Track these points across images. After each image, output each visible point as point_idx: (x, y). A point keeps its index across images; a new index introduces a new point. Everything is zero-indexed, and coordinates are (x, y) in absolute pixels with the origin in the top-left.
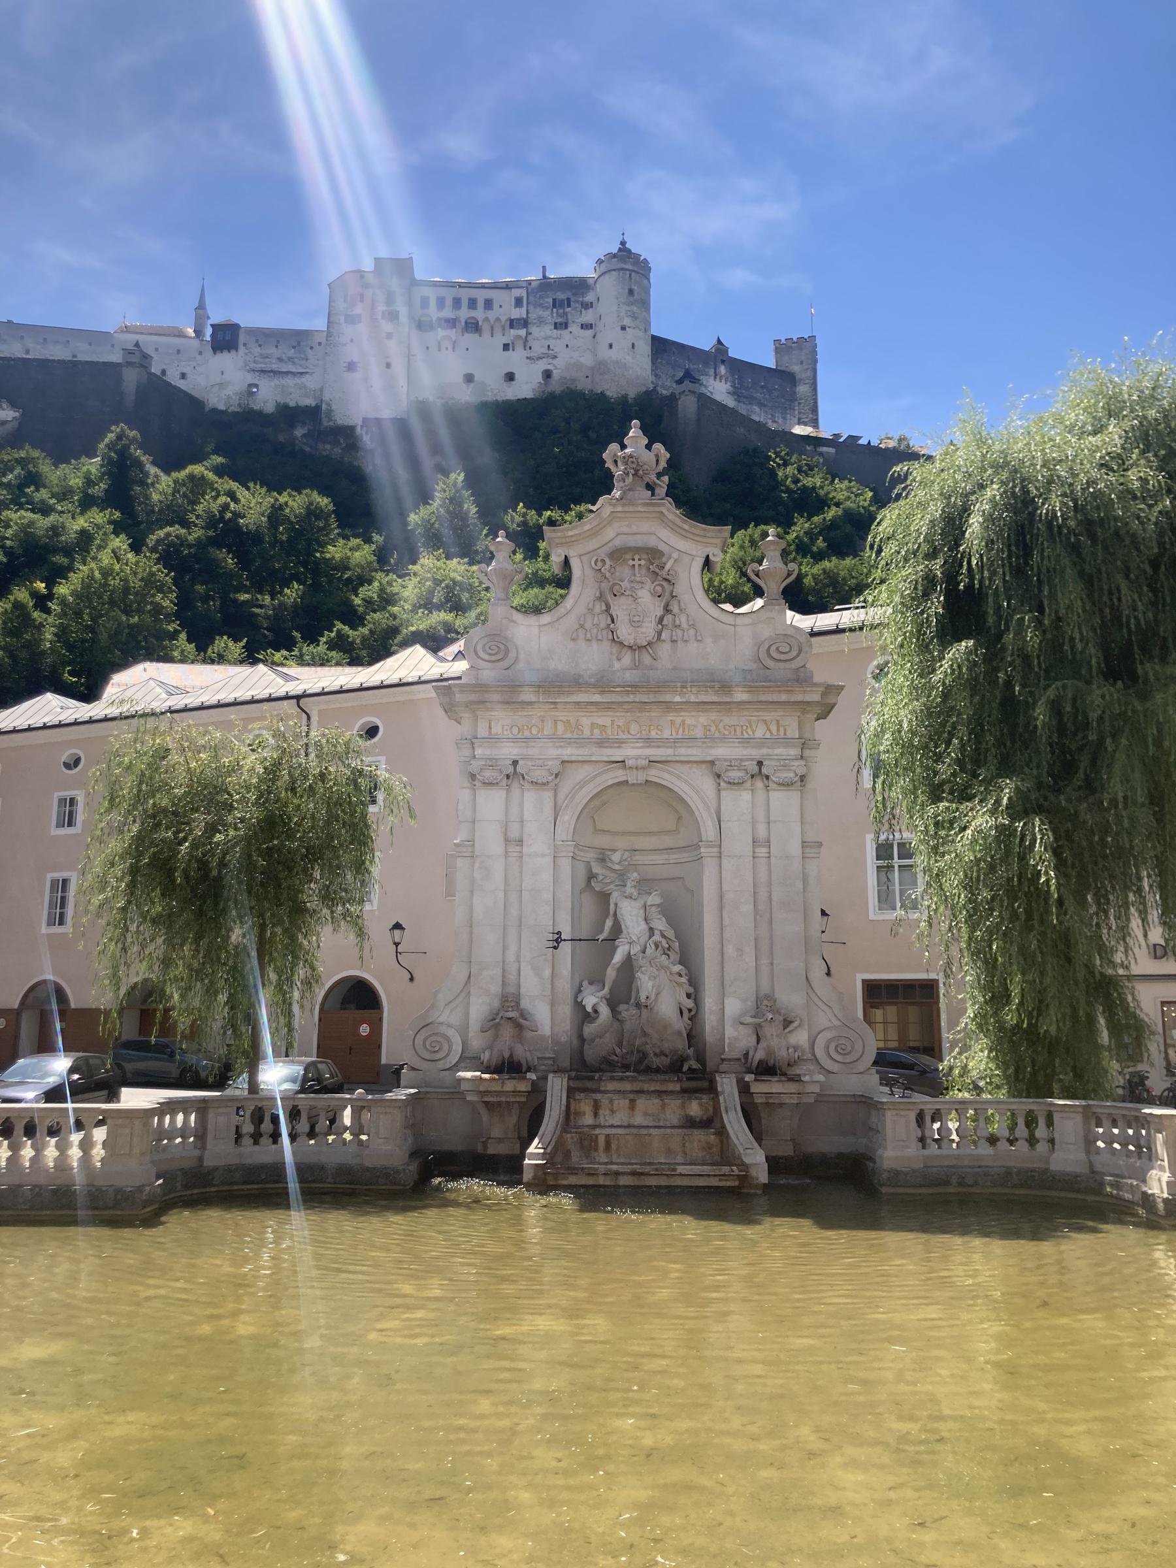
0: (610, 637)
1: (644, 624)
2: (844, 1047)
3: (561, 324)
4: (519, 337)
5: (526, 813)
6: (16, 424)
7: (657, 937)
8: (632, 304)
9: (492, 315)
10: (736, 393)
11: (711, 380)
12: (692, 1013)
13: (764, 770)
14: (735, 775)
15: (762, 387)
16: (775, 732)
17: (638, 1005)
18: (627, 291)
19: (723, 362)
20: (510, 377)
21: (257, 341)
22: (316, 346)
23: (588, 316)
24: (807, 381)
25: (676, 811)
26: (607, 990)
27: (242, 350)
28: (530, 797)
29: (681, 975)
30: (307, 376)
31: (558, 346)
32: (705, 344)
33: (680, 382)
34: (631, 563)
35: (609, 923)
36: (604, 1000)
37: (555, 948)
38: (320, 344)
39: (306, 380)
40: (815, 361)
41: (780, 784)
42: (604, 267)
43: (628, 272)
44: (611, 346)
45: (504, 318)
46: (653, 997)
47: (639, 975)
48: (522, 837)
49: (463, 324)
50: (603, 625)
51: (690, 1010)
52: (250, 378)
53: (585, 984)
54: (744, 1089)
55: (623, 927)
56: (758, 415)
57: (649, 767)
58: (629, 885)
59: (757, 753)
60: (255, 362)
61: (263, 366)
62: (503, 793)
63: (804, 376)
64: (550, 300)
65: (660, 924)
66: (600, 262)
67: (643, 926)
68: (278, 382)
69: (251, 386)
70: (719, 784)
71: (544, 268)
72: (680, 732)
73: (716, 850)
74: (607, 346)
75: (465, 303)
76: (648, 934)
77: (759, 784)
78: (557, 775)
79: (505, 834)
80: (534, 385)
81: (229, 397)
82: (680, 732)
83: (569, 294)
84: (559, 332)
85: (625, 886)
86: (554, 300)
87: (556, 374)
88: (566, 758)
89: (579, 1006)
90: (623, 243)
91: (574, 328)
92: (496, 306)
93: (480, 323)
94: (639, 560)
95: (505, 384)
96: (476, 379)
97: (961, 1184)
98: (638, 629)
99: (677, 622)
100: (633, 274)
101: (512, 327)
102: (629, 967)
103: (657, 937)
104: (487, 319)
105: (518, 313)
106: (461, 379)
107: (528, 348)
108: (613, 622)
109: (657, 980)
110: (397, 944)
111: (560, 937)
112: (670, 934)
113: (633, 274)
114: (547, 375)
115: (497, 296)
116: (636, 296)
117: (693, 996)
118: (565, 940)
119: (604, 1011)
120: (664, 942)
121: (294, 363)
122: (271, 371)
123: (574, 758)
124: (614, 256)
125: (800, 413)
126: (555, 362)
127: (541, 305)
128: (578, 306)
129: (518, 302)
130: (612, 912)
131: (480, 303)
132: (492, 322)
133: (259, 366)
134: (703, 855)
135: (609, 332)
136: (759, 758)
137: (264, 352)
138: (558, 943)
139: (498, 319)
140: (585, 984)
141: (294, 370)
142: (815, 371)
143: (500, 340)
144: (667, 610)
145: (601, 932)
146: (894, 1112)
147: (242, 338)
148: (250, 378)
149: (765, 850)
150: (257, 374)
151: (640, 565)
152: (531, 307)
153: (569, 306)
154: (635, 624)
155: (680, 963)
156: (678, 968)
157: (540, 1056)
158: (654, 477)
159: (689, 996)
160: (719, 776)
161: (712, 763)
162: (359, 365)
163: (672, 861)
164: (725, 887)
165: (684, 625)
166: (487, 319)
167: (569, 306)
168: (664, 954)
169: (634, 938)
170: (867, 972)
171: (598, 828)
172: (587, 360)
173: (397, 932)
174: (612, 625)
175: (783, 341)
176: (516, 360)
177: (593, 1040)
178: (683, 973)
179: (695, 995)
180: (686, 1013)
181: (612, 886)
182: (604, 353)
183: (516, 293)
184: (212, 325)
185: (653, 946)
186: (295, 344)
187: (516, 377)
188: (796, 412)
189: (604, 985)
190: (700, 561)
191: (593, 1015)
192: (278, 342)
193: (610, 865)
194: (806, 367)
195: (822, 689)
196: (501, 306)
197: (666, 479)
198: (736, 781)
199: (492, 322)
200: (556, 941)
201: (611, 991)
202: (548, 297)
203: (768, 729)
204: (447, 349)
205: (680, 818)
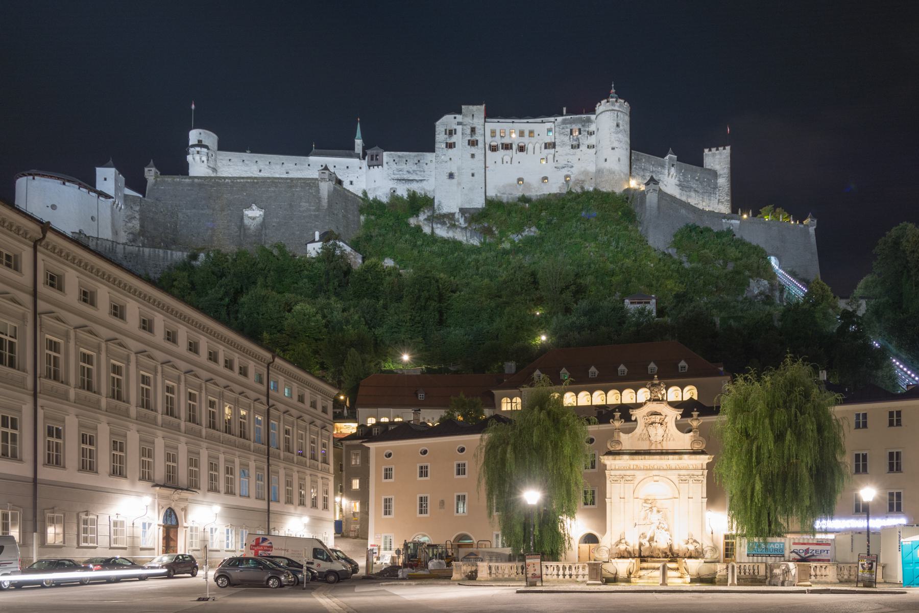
6: (262, 219)
8: (617, 133)
9: (533, 140)
10: (682, 186)
11: (666, 177)
15: (697, 180)
18: (615, 124)
21: (394, 161)
23: (592, 140)
24: (724, 176)
30: (425, 182)
31: (573, 160)
39: (424, 184)
44: (606, 160)
52: (393, 185)
60: (394, 174)
61: (398, 176)
63: (722, 172)
64: (569, 130)
68: (408, 187)
80: (560, 185)
81: (380, 196)
83: (580, 126)
91: (583, 148)
92: (536, 134)
101: (546, 148)
106: (516, 182)
116: (621, 127)
121: (417, 174)
122: (403, 180)
126: (572, 170)
131: (527, 133)
133: (396, 177)
135: (606, 152)
137: (398, 167)
148: (393, 185)
152: (557, 135)
172: (592, 168)
192: (407, 161)
202: (567, 128)
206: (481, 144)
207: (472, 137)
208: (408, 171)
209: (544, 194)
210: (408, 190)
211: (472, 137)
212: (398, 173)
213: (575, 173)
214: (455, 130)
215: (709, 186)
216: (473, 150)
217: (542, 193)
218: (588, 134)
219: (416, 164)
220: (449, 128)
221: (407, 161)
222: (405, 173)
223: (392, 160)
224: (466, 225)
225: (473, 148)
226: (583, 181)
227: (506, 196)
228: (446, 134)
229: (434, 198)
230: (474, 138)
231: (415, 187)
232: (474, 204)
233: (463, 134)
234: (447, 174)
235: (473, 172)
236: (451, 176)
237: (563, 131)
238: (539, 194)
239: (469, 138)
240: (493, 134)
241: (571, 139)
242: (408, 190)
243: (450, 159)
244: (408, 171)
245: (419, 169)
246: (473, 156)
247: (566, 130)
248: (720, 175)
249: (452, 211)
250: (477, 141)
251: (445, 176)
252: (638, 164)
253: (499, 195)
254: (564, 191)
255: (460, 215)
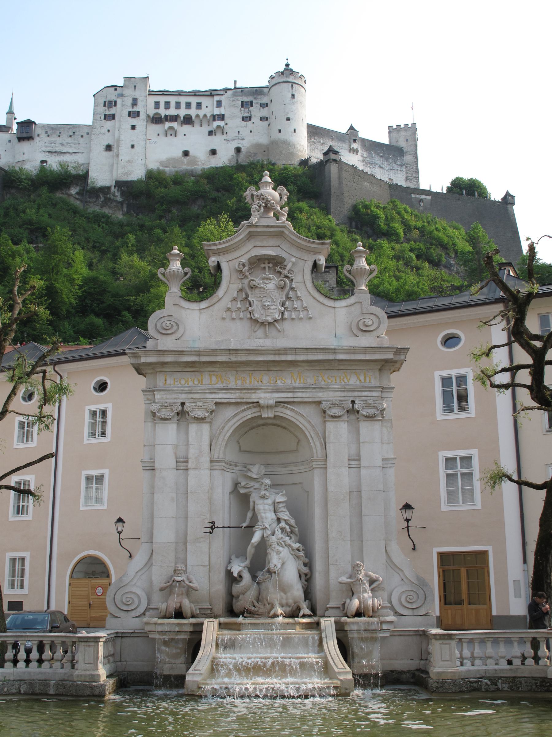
0: (249, 316)
1: (272, 307)
2: (411, 597)
3: (247, 117)
4: (219, 127)
5: (190, 439)
7: (283, 524)
12: (308, 577)
13: (356, 406)
14: (335, 411)
16: (363, 381)
17: (270, 572)
19: (355, 141)
20: (213, 152)
21: (47, 132)
22: (85, 135)
23: (264, 112)
24: (411, 153)
25: (296, 437)
26: (247, 562)
27: (37, 139)
28: (193, 428)
29: (298, 550)
30: (79, 155)
31: (245, 132)
32: (343, 129)
33: (326, 154)
34: (263, 266)
35: (249, 515)
36: (246, 569)
37: (210, 533)
38: (88, 133)
40: (415, 140)
41: (367, 417)
42: (274, 81)
43: (290, 84)
45: (208, 116)
46: (279, 566)
47: (269, 551)
48: (187, 456)
49: (182, 118)
50: (243, 309)
51: (306, 575)
53: (233, 557)
54: (340, 629)
55: (259, 517)
56: (380, 174)
57: (275, 406)
58: (263, 489)
59: (352, 395)
60: (46, 147)
62: (175, 426)
63: (409, 150)
65: (285, 515)
66: (272, 78)
67: (274, 516)
69: (43, 162)
70: (325, 417)
71: (235, 82)
72: (298, 381)
73: (323, 463)
74: (278, 131)
75: (183, 105)
76: (276, 522)
77: (353, 417)
78: (212, 412)
79: (175, 453)
82: (298, 381)
84: (245, 123)
85: (260, 489)
86: (242, 103)
87: (243, 150)
88: (218, 400)
89: (229, 573)
90: (287, 65)
91: (255, 119)
92: (204, 106)
93: (193, 118)
94: (269, 263)
95: (211, 157)
96: (191, 154)
97: (487, 691)
98: (267, 311)
99: (296, 306)
100: (294, 85)
101: (214, 120)
102: (263, 546)
103: (283, 524)
104: (197, 116)
105: (217, 111)
106: (180, 154)
107: (225, 133)
108: (251, 306)
109: (281, 555)
110: (120, 533)
111: (214, 525)
112: (292, 522)
113: (294, 85)
114: (238, 150)
115: (205, 101)
117: (309, 565)
118: (217, 527)
119: (247, 576)
120: (287, 527)
122: (55, 152)
123: (223, 400)
124: (282, 73)
125: (407, 173)
126: (244, 142)
127: (234, 106)
128: (259, 106)
129: (219, 104)
130: (251, 507)
131: (194, 105)
132: (201, 116)
134: (314, 466)
136: (352, 399)
138: (213, 529)
139: (205, 116)
140: (233, 557)
141: (70, 151)
142: (416, 146)
143: (206, 129)
144: (288, 298)
145: (244, 521)
146: (441, 641)
147: (38, 131)
149: (356, 462)
150: (47, 154)
151: (269, 267)
153: (252, 106)
154: (265, 308)
155: (299, 542)
156: (297, 545)
157: (200, 607)
158: (278, 208)
159: (305, 565)
160: (324, 412)
161: (320, 402)
162: (113, 147)
163: (294, 472)
164: (331, 488)
165: (300, 309)
166: (197, 116)
167: (252, 106)
168: (288, 536)
169: (267, 526)
170: (440, 546)
171: (242, 449)
172: (264, 140)
173: (120, 524)
174: (250, 308)
175: (395, 127)
176: (217, 142)
177: (238, 597)
178: (301, 549)
179: (309, 564)
180: (303, 577)
181: (251, 489)
182: (275, 136)
183: (217, 98)
184: (18, 123)
185: (280, 531)
186: (71, 134)
187: (217, 152)
188: (404, 173)
189: (246, 559)
190: (310, 264)
191: (238, 579)
192: (60, 133)
193: (249, 474)
194: (411, 143)
195: (395, 350)
196: (207, 107)
197: (287, 209)
198: (336, 415)
199: (201, 116)
200: (211, 528)
201: (252, 562)
203: (358, 378)
204: (171, 135)
205: (299, 441)
206: (142, 115)
207: (133, 108)
208: (61, 144)
209: (213, 168)
210: (60, 163)
211: (133, 108)
212: (49, 145)
213: (245, 145)
214: (115, 102)
215: (395, 163)
216: (134, 121)
217: (210, 166)
218: (261, 106)
219: (71, 136)
220: (109, 99)
221: (60, 133)
222: (57, 145)
223: (44, 132)
224: (121, 200)
225: (133, 120)
226: (255, 154)
227: (168, 169)
228: (105, 105)
229: (87, 172)
230: (136, 109)
231: (67, 158)
232: (132, 176)
233: (123, 105)
234: (104, 147)
235: (133, 143)
236: (109, 148)
237: (234, 103)
238: (206, 167)
239: (131, 110)
240: (157, 105)
241: (243, 112)
242: (60, 163)
243: (109, 131)
244: (61, 144)
245: (73, 141)
246: (133, 127)
247: (237, 102)
248: (407, 152)
249: (107, 184)
250: (138, 112)
251: (102, 148)
252: (316, 138)
253: (161, 168)
254: (233, 163)
255: (117, 188)
